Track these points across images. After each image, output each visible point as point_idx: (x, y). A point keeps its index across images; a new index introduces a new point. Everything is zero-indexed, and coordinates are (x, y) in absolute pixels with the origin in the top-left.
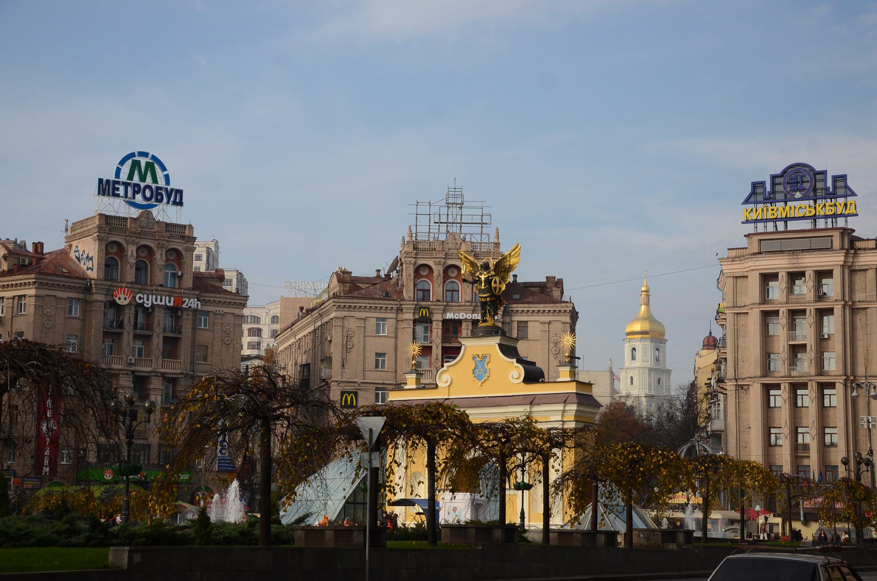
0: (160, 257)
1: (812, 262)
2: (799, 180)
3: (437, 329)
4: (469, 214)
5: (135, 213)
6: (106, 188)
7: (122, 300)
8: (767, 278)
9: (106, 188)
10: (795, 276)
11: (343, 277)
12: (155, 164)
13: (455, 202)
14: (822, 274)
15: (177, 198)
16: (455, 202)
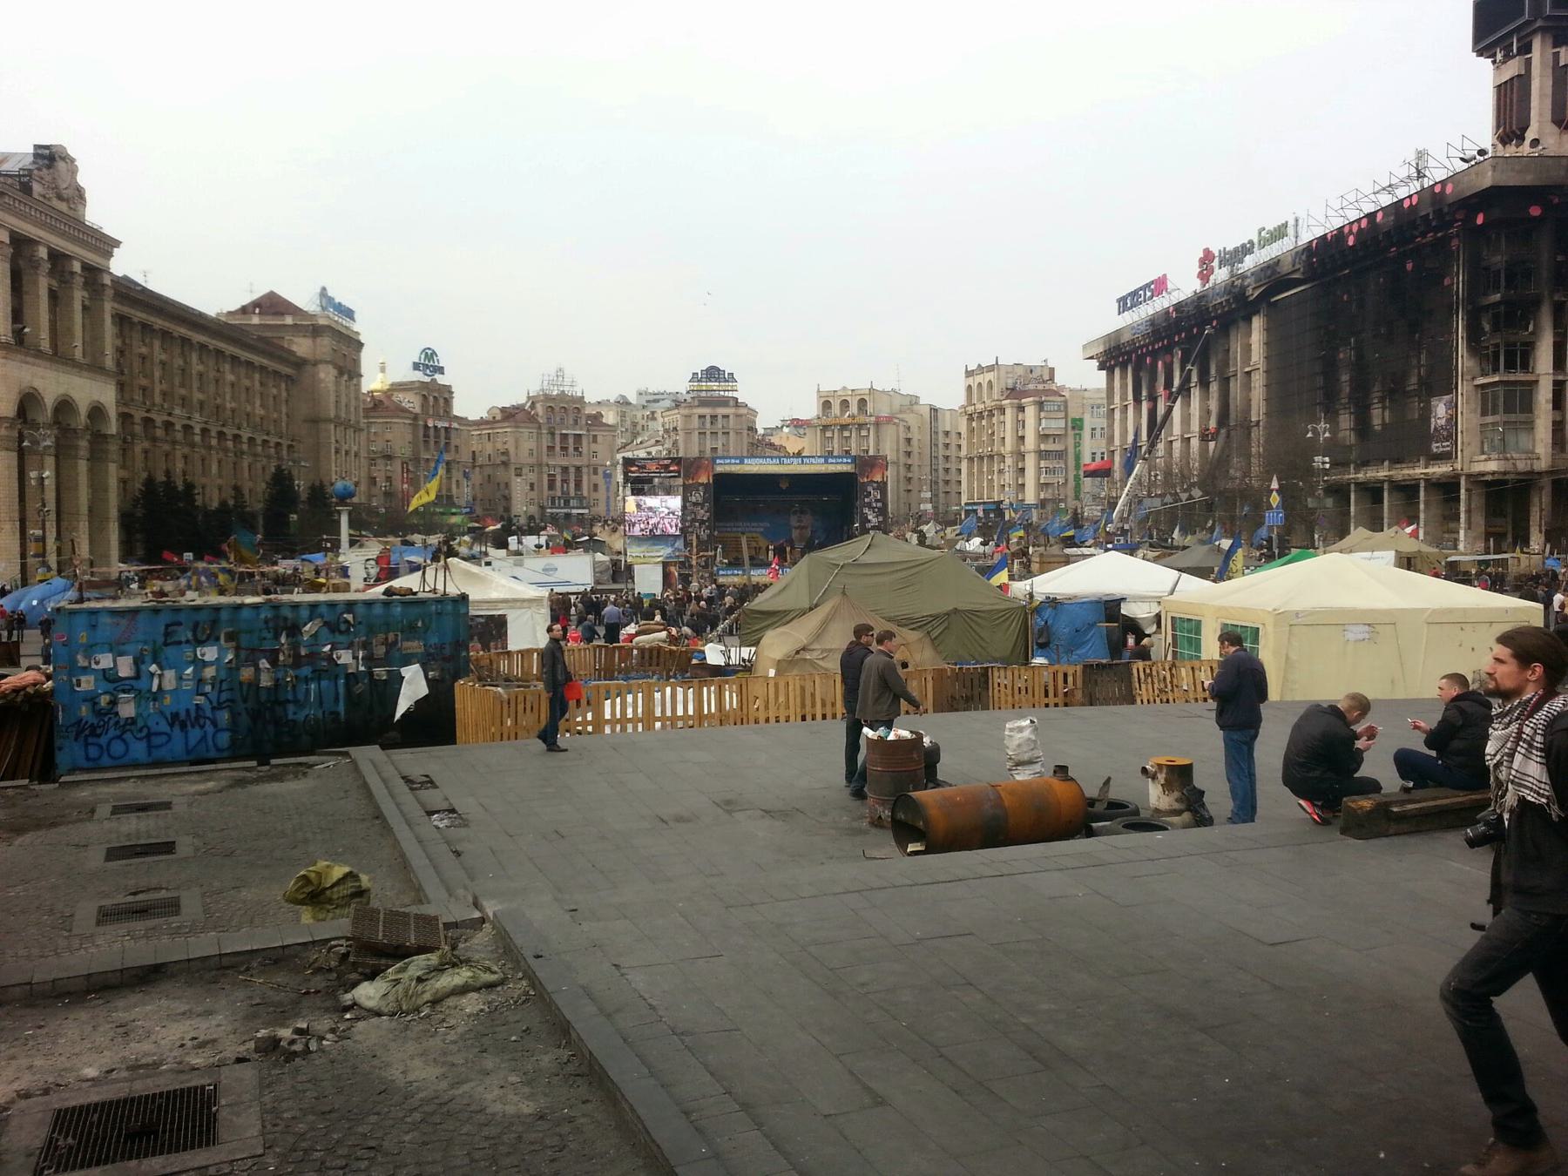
0: (441, 401)
1: (721, 411)
2: (713, 373)
3: (558, 438)
4: (567, 381)
5: (427, 379)
6: (416, 366)
7: (430, 424)
8: (702, 417)
9: (416, 366)
10: (714, 417)
11: (503, 410)
12: (434, 353)
13: (560, 372)
14: (726, 417)
15: (441, 370)
16: (560, 372)
